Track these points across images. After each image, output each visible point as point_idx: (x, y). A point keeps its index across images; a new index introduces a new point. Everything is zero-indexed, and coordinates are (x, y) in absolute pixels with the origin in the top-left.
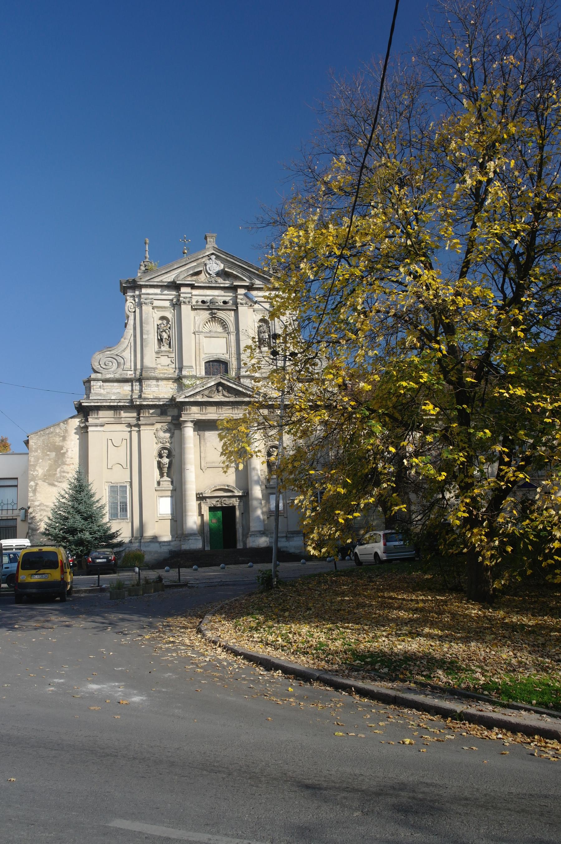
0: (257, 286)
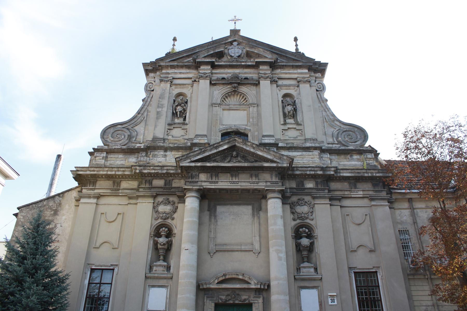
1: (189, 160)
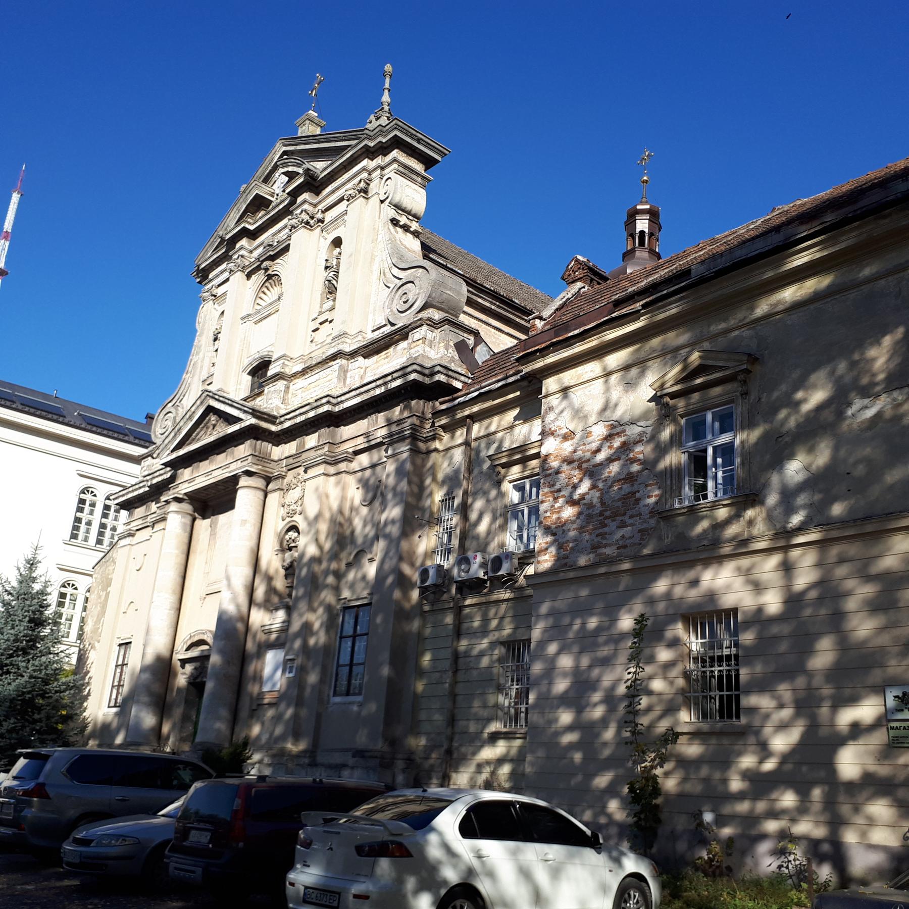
0: (323, 175)
1: (168, 452)
